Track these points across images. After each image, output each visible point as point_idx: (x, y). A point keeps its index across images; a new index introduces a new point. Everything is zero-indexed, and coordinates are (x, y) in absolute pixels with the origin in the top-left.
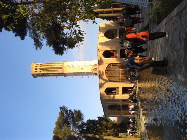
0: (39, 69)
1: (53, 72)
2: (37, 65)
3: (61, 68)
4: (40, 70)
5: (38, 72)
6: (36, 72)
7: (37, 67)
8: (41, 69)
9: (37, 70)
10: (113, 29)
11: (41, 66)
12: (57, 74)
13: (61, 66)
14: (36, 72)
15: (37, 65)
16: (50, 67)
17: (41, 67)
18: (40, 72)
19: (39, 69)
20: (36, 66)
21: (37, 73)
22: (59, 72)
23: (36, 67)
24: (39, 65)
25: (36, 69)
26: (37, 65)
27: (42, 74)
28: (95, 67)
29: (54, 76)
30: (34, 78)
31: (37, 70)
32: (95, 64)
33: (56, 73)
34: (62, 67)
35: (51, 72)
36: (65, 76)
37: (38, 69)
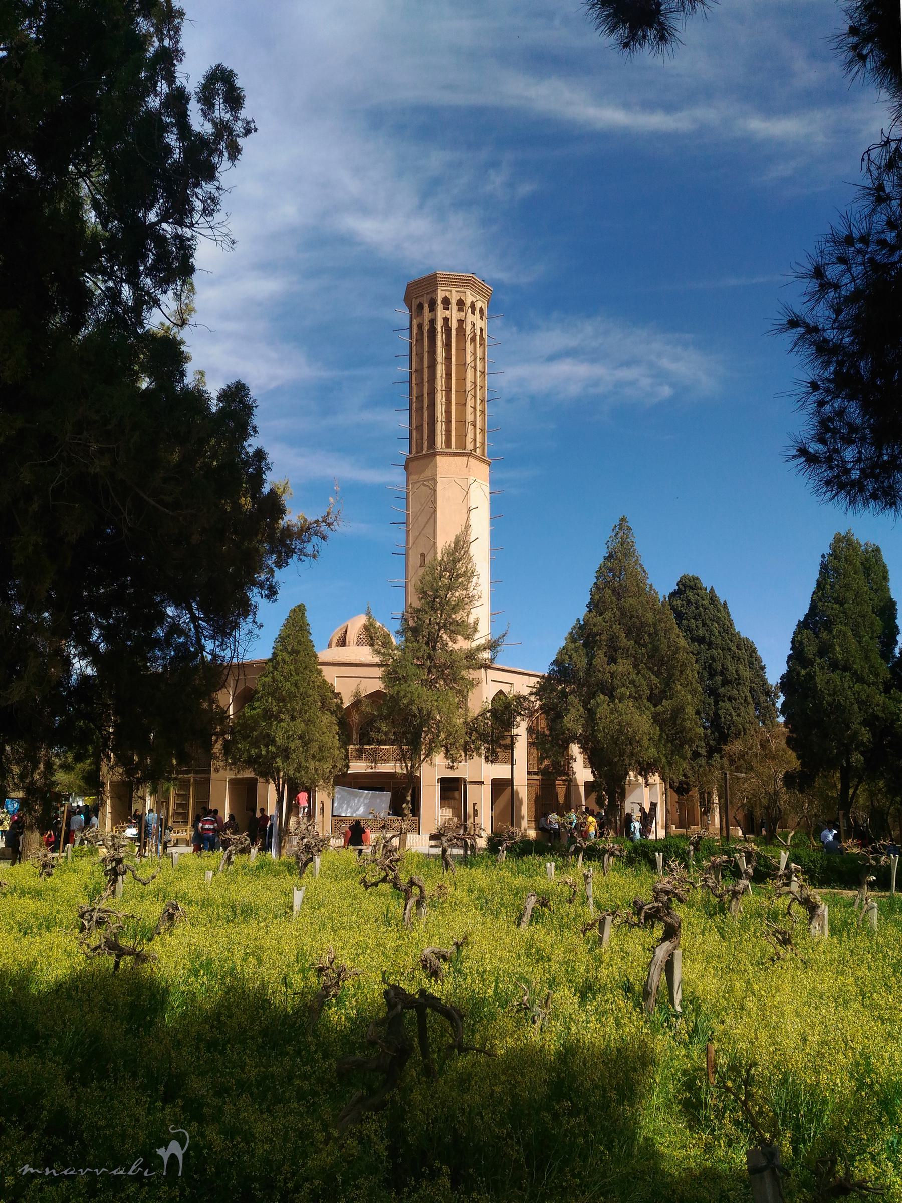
0: (461, 322)
3: (462, 444)
4: (454, 325)
6: (447, 302)
9: (454, 307)
15: (477, 312)
19: (461, 322)
20: (473, 306)
21: (440, 306)
23: (468, 304)
24: (480, 324)
25: (461, 304)
30: (410, 286)
31: (454, 307)
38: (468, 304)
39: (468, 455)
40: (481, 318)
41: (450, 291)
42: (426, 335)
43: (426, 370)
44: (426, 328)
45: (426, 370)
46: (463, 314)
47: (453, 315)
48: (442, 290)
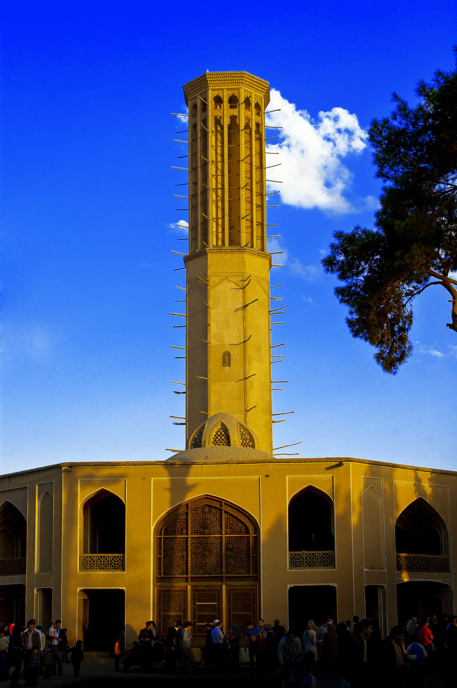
0: (233, 119)
1: (212, 196)
2: (257, 106)
4: (226, 122)
5: (218, 113)
7: (243, 106)
8: (230, 128)
10: (447, 553)
11: (247, 126)
12: (200, 214)
13: (244, 238)
14: (218, 100)
16: (243, 181)
17: (242, 126)
18: (218, 122)
19: (233, 119)
20: (247, 102)
22: (212, 226)
23: (242, 100)
25: (233, 101)
26: (257, 106)
27: (205, 135)
28: (235, 438)
29: (194, 196)
32: (252, 439)
33: (205, 210)
34: (243, 243)
35: (212, 183)
36: (187, 259)
37: (234, 112)
38: (242, 100)
39: (242, 250)
40: (258, 114)
41: (222, 90)
42: (199, 135)
43: (199, 170)
44: (199, 128)
45: (199, 170)
46: (237, 109)
47: (225, 112)
48: (213, 90)
